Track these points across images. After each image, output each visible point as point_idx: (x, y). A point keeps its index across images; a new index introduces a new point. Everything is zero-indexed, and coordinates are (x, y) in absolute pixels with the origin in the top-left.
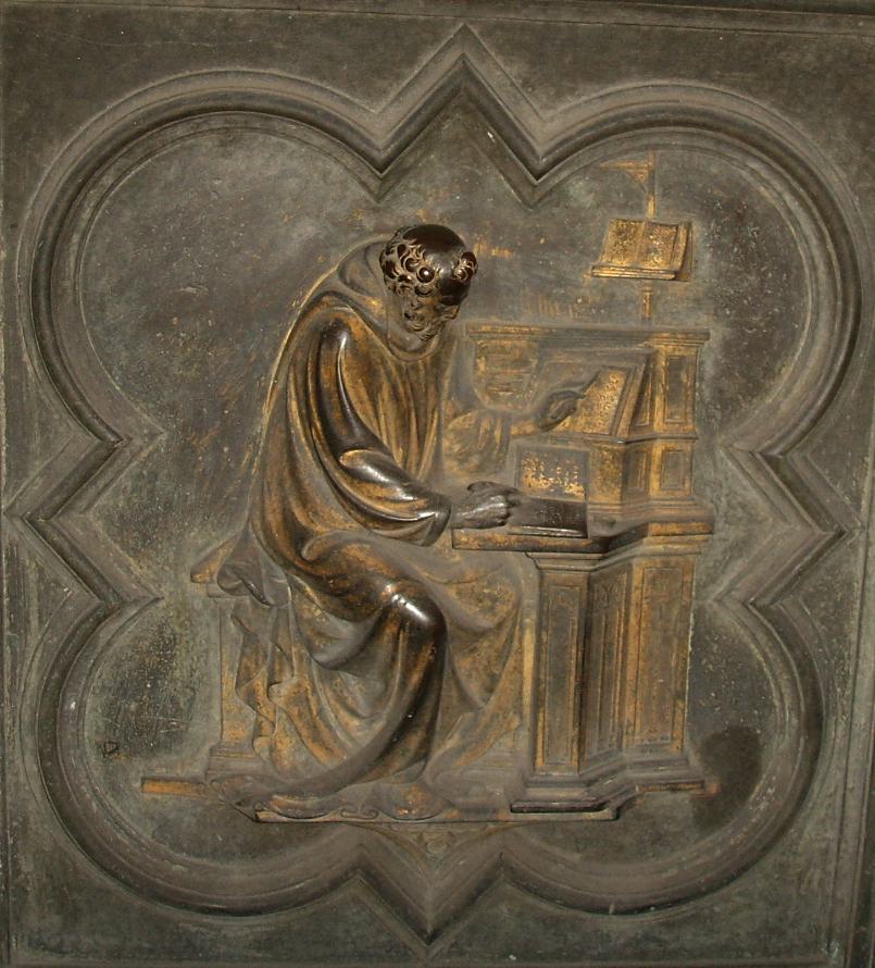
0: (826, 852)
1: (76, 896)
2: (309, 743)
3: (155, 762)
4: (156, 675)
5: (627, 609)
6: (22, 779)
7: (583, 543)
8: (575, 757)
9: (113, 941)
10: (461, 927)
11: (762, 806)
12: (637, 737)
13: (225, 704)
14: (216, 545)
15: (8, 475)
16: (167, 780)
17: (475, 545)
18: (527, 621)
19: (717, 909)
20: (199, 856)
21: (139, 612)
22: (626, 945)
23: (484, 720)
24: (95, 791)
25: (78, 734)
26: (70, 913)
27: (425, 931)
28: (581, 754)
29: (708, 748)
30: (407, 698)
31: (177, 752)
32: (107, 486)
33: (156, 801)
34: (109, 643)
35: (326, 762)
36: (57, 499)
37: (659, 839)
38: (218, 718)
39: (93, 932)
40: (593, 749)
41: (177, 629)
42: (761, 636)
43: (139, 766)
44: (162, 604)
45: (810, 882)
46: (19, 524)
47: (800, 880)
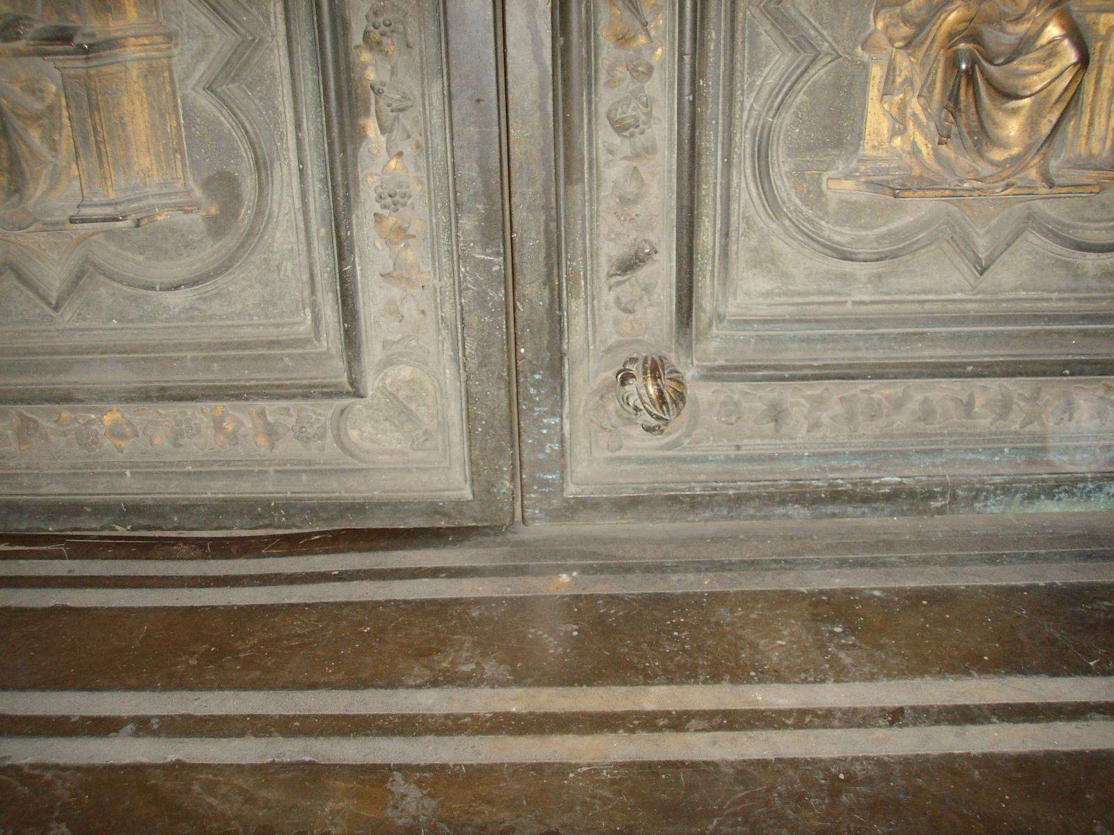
0: (292, 251)
11: (246, 222)
22: (180, 313)
37: (187, 245)
45: (286, 271)
47: (280, 270)
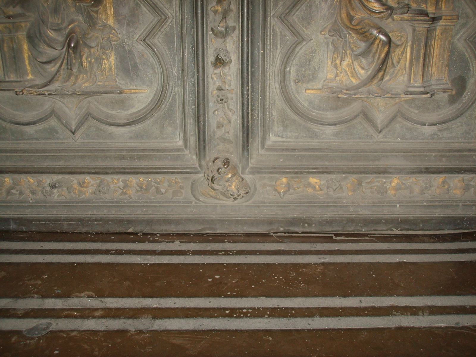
1: (287, 122)
2: (351, 78)
3: (309, 85)
4: (310, 61)
5: (435, 41)
6: (274, 90)
7: (427, 18)
8: (421, 80)
9: (297, 134)
10: (387, 130)
11: (466, 98)
12: (435, 77)
13: (328, 68)
14: (327, 24)
15: (273, 6)
16: (312, 89)
17: (399, 19)
18: (408, 44)
19: (453, 126)
20: (319, 111)
21: (306, 43)
22: (428, 136)
23: (396, 71)
24: (293, 93)
25: (289, 77)
26: (285, 127)
27: (378, 130)
28: (423, 79)
29: (453, 81)
30: (380, 61)
31: (315, 82)
32: (299, 9)
33: (309, 96)
34: (298, 52)
35: (355, 82)
36: (287, 11)
38: (326, 72)
39: (291, 132)
40: (425, 79)
41: (316, 48)
42: (469, 50)
43: (305, 86)
44: (312, 41)
46: (276, 19)
